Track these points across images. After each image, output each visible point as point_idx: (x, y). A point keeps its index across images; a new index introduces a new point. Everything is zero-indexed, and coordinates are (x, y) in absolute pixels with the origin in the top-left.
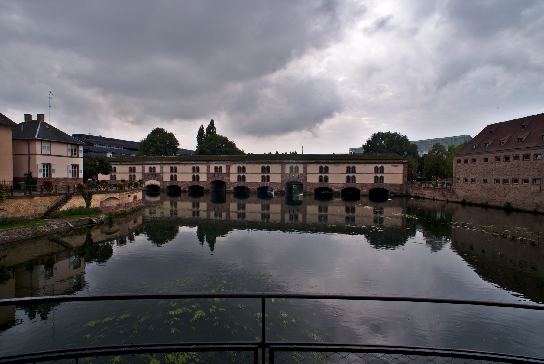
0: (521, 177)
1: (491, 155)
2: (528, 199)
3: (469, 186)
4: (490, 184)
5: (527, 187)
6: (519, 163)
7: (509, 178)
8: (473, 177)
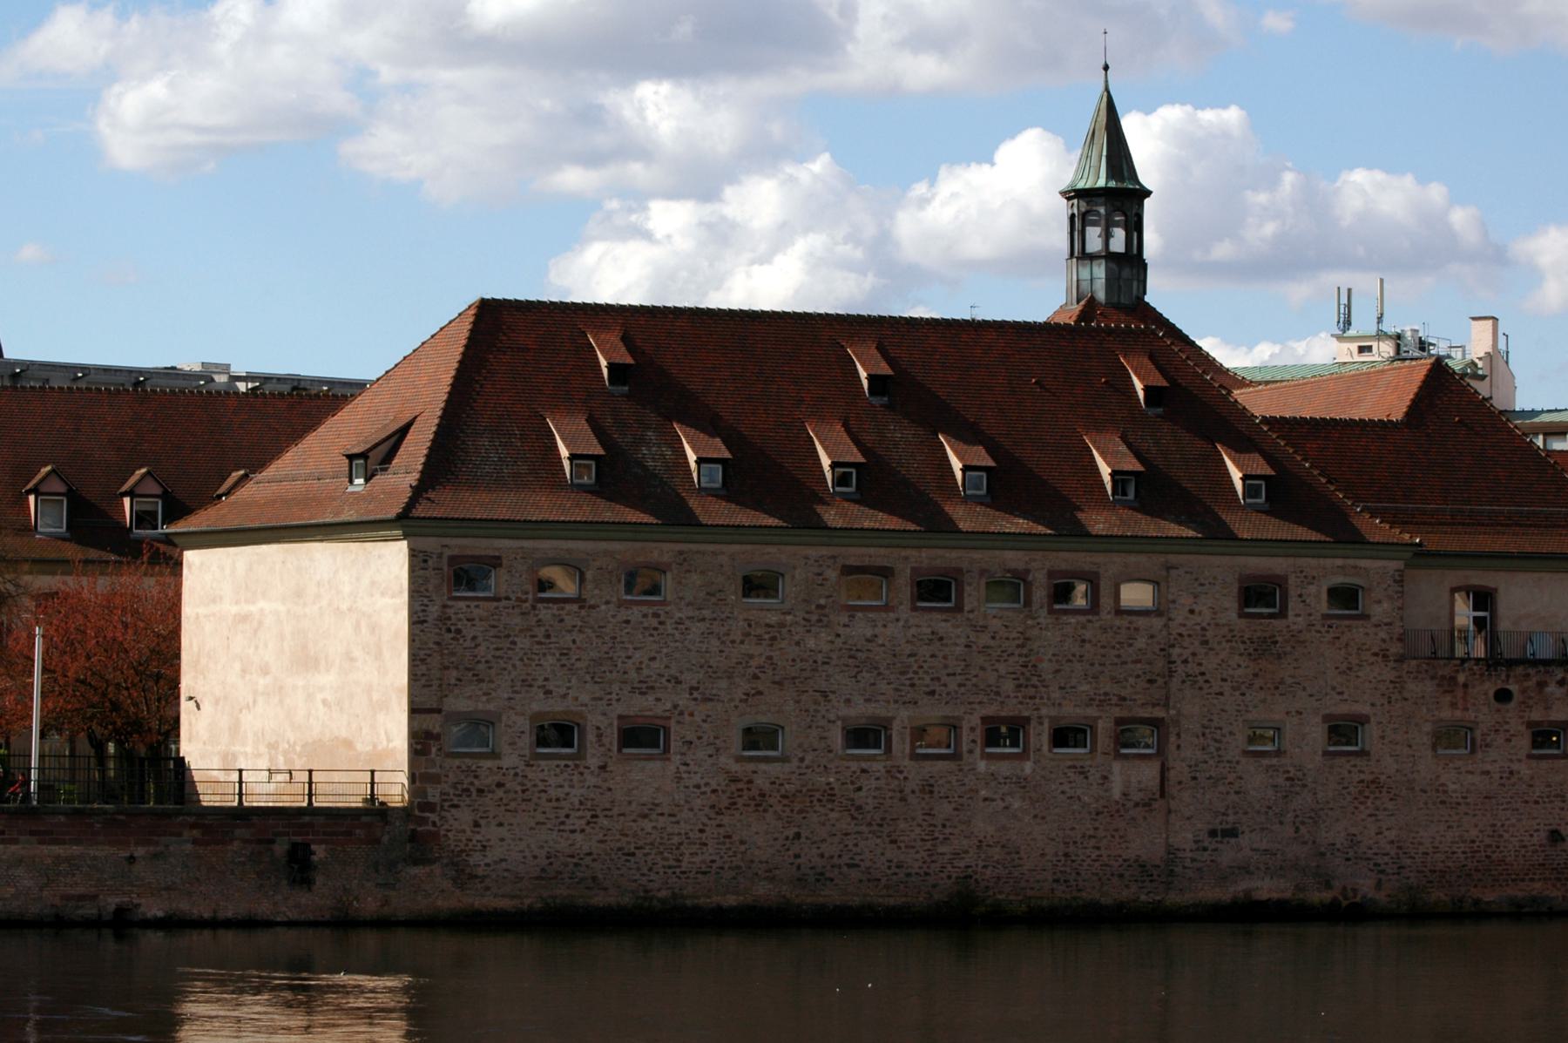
0: (1044, 711)
1: (813, 552)
2: (1093, 842)
3: (591, 780)
4: (809, 758)
5: (1084, 773)
6: (1030, 622)
7: (960, 719)
8: (641, 706)
